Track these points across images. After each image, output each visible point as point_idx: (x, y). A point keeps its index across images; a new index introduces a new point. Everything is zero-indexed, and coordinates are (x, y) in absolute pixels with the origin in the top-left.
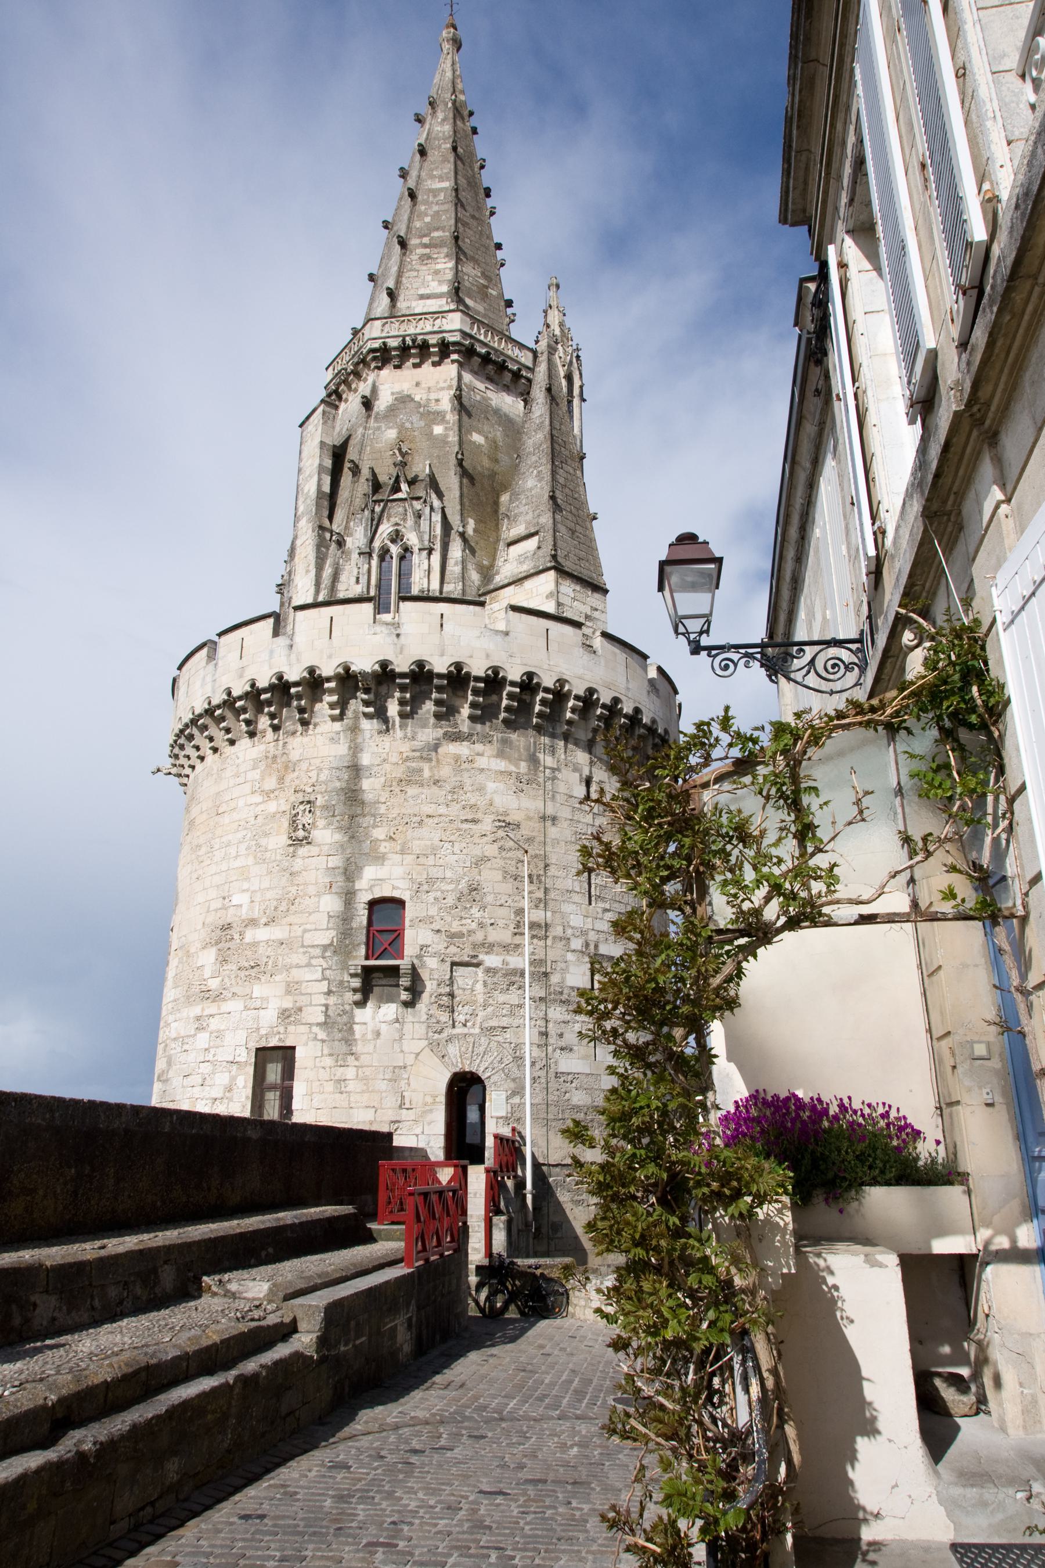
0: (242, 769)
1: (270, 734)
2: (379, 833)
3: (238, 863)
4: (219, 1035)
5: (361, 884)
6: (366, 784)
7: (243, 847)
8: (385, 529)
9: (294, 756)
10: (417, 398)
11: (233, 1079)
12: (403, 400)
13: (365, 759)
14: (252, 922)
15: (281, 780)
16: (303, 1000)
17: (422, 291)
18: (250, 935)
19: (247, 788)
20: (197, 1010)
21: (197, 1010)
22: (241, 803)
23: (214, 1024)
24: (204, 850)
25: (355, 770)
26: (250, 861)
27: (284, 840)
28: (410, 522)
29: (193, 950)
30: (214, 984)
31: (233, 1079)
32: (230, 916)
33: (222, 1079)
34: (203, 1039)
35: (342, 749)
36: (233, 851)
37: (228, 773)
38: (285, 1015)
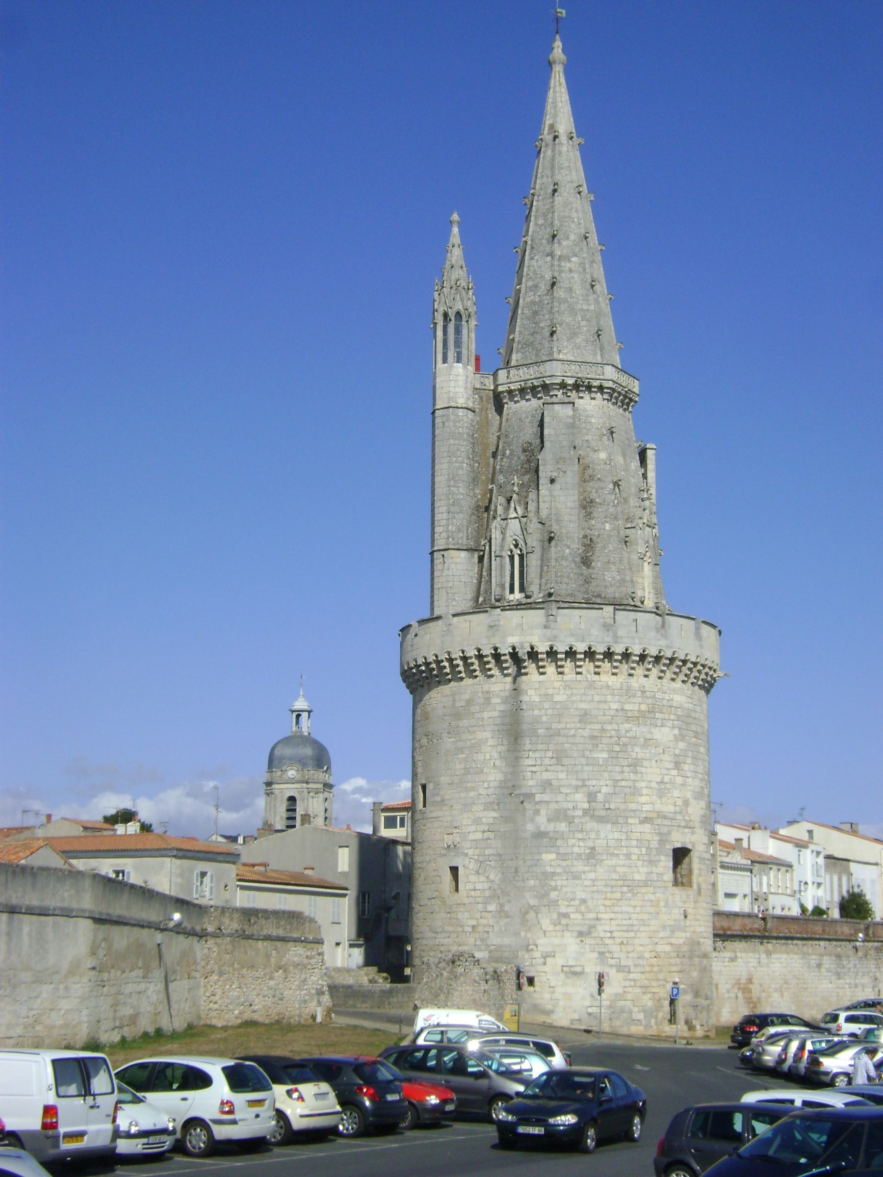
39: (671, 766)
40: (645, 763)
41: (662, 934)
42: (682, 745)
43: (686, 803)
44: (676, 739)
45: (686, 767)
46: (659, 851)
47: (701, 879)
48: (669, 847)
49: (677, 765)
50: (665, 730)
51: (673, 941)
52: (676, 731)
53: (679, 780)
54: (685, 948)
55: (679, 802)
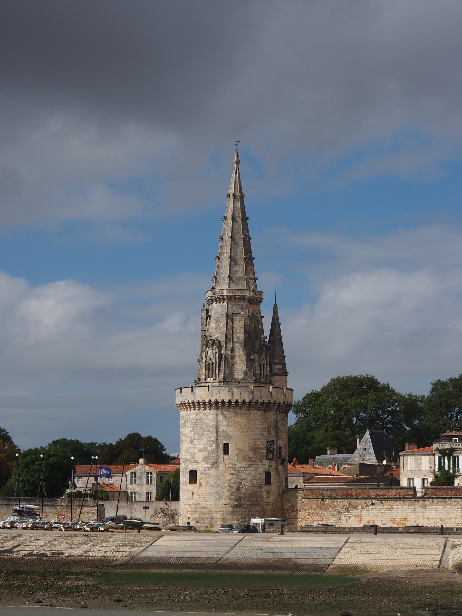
0: (256, 416)
1: (263, 411)
2: (280, 434)
3: (258, 436)
4: (257, 468)
5: (278, 444)
6: (278, 424)
7: (258, 433)
8: (262, 358)
9: (268, 416)
10: (255, 314)
11: (261, 477)
12: (253, 314)
13: (278, 420)
14: (262, 448)
15: (266, 421)
16: (272, 464)
17: (250, 276)
18: (261, 451)
19: (258, 421)
20: (250, 463)
21: (250, 463)
22: (257, 423)
23: (255, 466)
24: (244, 430)
25: (277, 422)
26: (260, 436)
27: (267, 433)
28: (265, 357)
29: (245, 451)
30: (254, 459)
31: (261, 477)
32: (256, 446)
33: (258, 476)
34: (252, 469)
35: (275, 417)
36: (256, 433)
37: (252, 416)
38: (269, 466)
39: (189, 441)
40: (184, 442)
41: (186, 501)
42: (193, 433)
43: (194, 454)
44: (191, 431)
45: (195, 441)
46: (186, 472)
47: (201, 481)
48: (188, 470)
49: (191, 441)
50: (188, 429)
51: (188, 503)
52: (191, 429)
53: (192, 446)
54: (192, 506)
55: (192, 454)
